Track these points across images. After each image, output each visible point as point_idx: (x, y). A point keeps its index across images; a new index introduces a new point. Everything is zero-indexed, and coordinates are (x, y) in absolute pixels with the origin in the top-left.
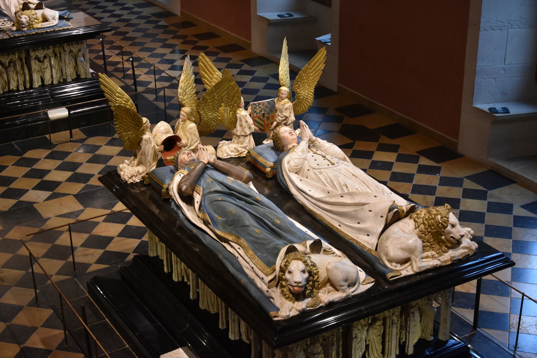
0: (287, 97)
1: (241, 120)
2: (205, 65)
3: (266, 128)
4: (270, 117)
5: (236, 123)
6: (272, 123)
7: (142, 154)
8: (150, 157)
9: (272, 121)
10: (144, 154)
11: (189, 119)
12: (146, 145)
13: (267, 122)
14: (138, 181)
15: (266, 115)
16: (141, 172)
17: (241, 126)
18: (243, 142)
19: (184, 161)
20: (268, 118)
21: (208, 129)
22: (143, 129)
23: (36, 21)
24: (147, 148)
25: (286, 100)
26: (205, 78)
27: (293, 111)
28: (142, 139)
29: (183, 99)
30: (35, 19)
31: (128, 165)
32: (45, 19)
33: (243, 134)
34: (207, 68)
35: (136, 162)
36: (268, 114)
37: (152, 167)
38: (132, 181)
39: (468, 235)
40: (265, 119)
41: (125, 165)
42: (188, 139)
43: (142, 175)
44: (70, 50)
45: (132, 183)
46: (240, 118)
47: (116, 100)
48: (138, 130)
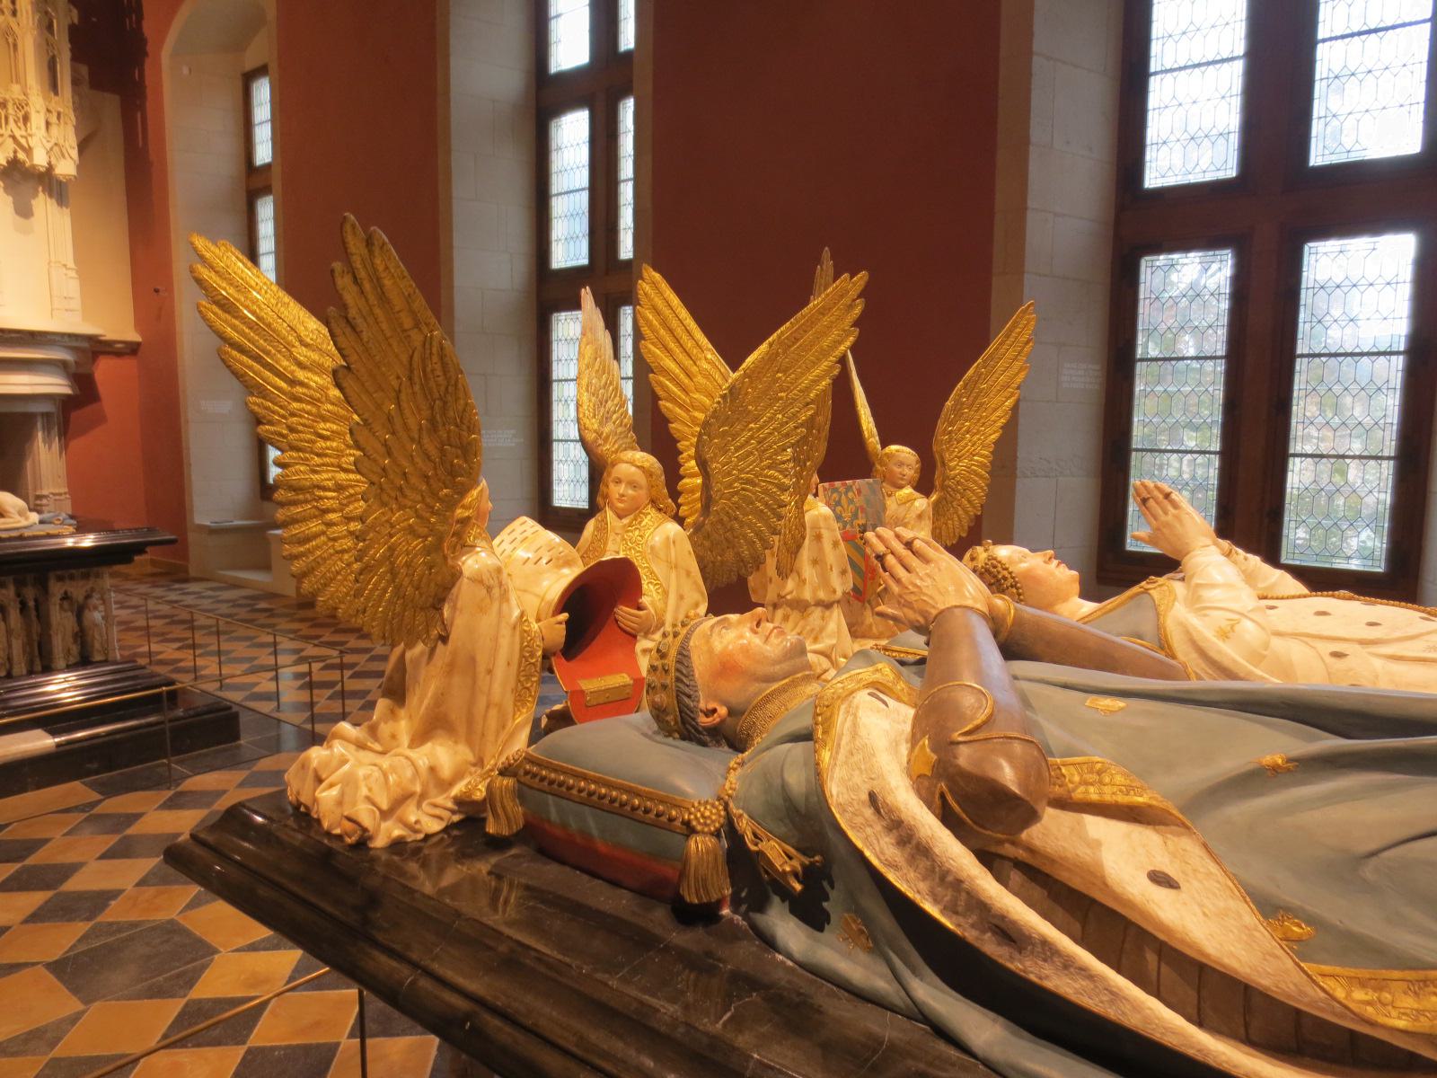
0: (909, 483)
1: (818, 537)
2: (665, 324)
5: (799, 547)
7: (451, 668)
8: (500, 679)
10: (467, 666)
11: (653, 502)
12: (482, 609)
14: (434, 826)
16: (446, 771)
17: (815, 562)
18: (822, 629)
19: (744, 662)
21: (730, 556)
22: (465, 522)
24: (486, 622)
25: (908, 490)
26: (665, 372)
28: (456, 575)
29: (600, 435)
31: (361, 746)
33: (822, 595)
34: (671, 331)
35: (403, 727)
37: (512, 735)
38: (397, 832)
41: (338, 748)
42: (666, 593)
43: (458, 789)
45: (397, 845)
46: (815, 527)
47: (293, 382)
48: (451, 504)
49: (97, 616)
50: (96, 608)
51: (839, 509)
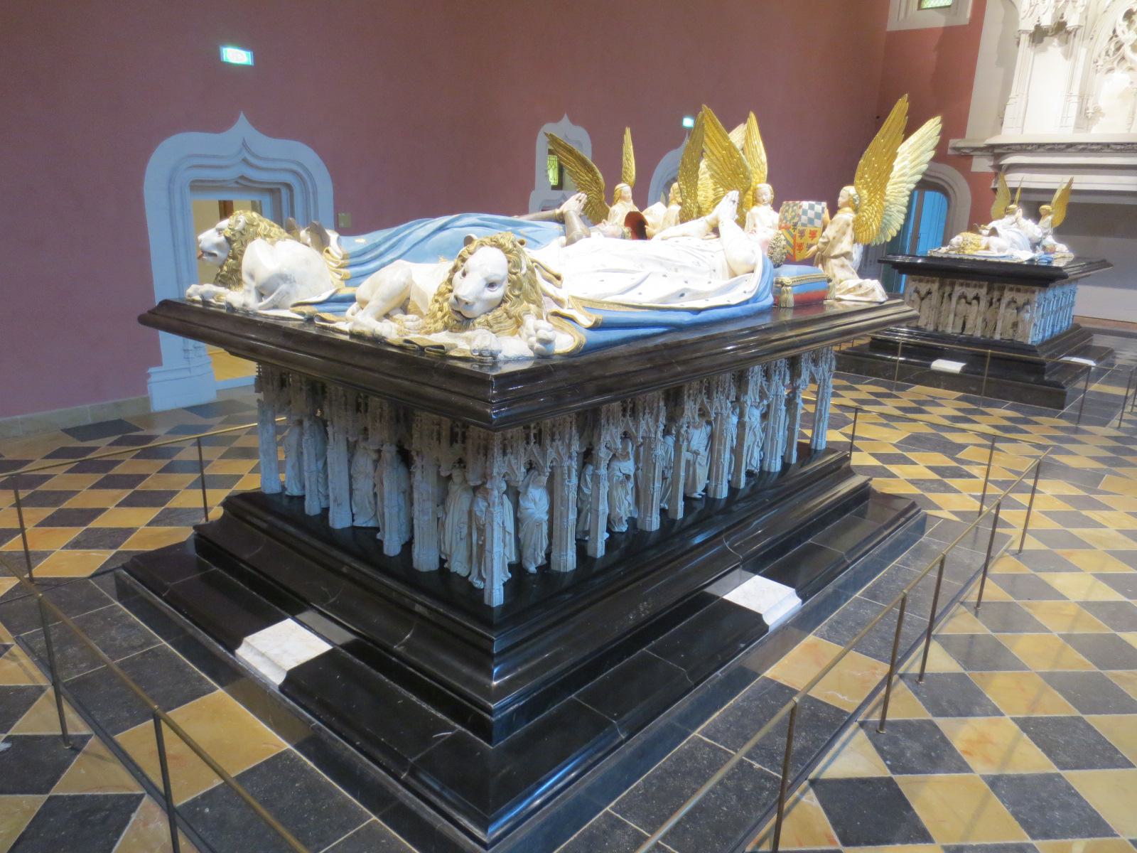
3: (797, 252)
4: (807, 234)
6: (810, 246)
9: (810, 242)
13: (798, 240)
15: (799, 227)
20: (802, 234)
23: (973, 246)
25: (848, 209)
27: (850, 231)
30: (971, 243)
32: (987, 248)
36: (804, 225)
39: (530, 336)
40: (796, 233)
44: (1013, 298)
49: (1027, 316)
50: (1027, 311)
51: (786, 214)
